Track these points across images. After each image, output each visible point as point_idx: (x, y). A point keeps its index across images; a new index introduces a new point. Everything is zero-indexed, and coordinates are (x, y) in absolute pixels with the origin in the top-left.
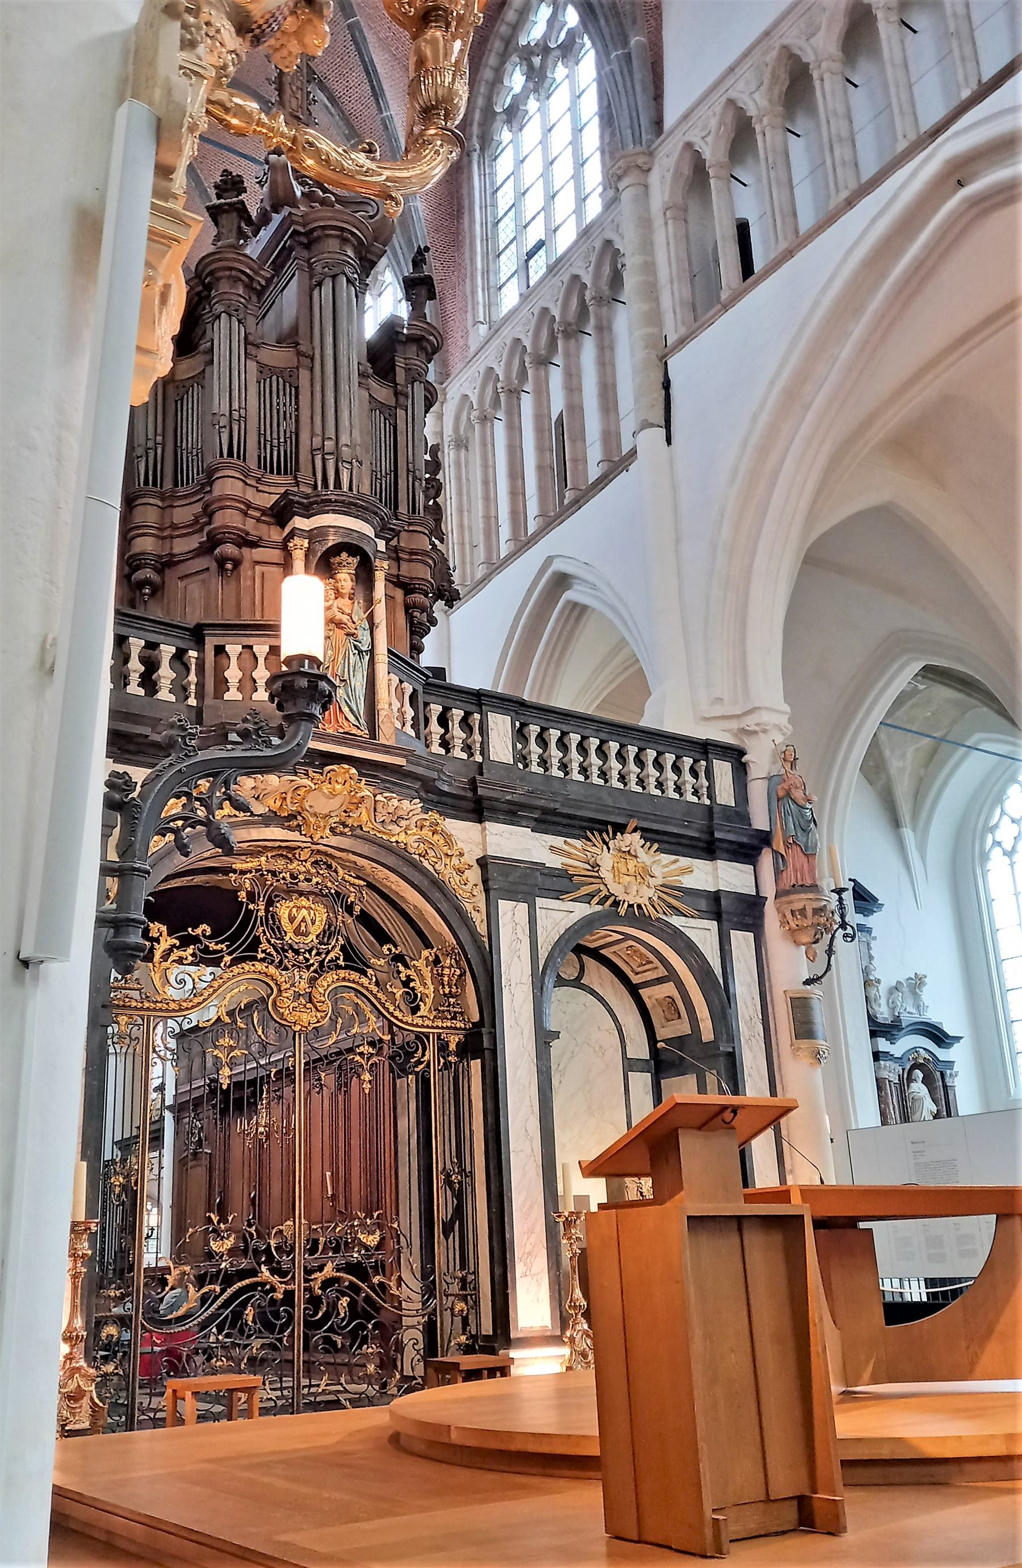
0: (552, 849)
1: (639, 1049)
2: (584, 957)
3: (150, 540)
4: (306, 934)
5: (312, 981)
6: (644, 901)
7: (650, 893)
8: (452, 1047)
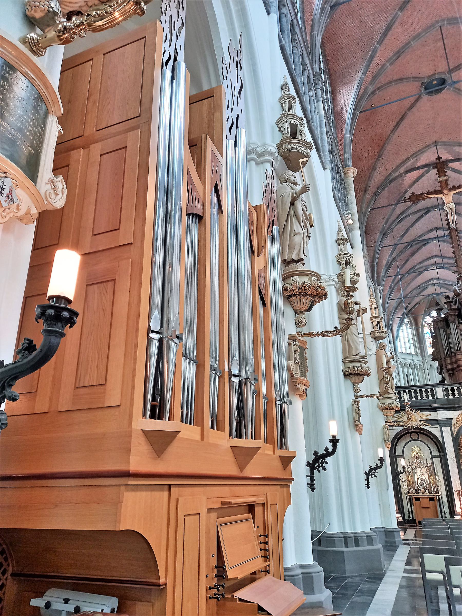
3: (450, 366)
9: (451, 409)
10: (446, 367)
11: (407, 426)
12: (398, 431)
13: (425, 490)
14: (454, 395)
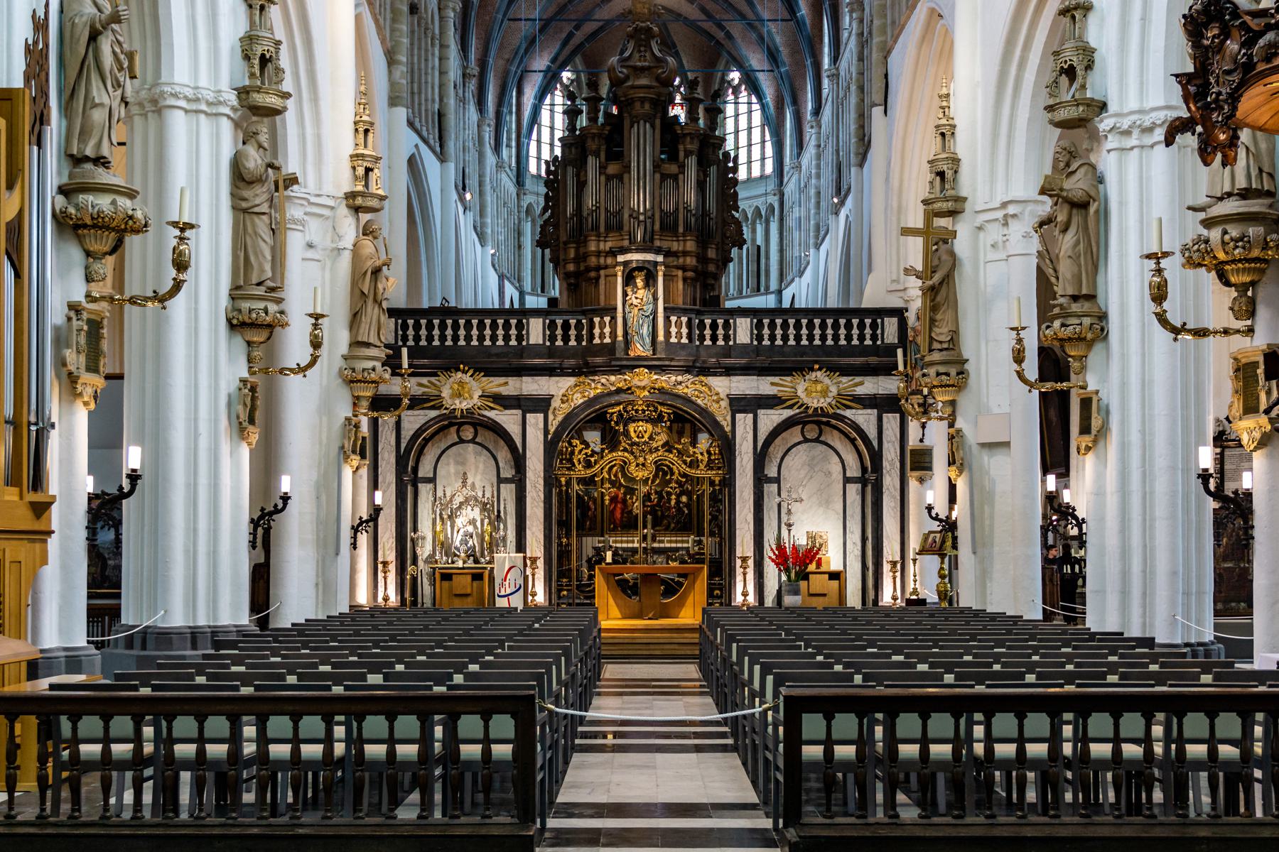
0: (772, 384)
1: (855, 471)
2: (823, 427)
4: (643, 437)
5: (645, 459)
6: (825, 405)
7: (829, 400)
8: (717, 482)
10: (564, 267)
11: (446, 409)
12: (427, 419)
13: (468, 557)
14: (566, 338)
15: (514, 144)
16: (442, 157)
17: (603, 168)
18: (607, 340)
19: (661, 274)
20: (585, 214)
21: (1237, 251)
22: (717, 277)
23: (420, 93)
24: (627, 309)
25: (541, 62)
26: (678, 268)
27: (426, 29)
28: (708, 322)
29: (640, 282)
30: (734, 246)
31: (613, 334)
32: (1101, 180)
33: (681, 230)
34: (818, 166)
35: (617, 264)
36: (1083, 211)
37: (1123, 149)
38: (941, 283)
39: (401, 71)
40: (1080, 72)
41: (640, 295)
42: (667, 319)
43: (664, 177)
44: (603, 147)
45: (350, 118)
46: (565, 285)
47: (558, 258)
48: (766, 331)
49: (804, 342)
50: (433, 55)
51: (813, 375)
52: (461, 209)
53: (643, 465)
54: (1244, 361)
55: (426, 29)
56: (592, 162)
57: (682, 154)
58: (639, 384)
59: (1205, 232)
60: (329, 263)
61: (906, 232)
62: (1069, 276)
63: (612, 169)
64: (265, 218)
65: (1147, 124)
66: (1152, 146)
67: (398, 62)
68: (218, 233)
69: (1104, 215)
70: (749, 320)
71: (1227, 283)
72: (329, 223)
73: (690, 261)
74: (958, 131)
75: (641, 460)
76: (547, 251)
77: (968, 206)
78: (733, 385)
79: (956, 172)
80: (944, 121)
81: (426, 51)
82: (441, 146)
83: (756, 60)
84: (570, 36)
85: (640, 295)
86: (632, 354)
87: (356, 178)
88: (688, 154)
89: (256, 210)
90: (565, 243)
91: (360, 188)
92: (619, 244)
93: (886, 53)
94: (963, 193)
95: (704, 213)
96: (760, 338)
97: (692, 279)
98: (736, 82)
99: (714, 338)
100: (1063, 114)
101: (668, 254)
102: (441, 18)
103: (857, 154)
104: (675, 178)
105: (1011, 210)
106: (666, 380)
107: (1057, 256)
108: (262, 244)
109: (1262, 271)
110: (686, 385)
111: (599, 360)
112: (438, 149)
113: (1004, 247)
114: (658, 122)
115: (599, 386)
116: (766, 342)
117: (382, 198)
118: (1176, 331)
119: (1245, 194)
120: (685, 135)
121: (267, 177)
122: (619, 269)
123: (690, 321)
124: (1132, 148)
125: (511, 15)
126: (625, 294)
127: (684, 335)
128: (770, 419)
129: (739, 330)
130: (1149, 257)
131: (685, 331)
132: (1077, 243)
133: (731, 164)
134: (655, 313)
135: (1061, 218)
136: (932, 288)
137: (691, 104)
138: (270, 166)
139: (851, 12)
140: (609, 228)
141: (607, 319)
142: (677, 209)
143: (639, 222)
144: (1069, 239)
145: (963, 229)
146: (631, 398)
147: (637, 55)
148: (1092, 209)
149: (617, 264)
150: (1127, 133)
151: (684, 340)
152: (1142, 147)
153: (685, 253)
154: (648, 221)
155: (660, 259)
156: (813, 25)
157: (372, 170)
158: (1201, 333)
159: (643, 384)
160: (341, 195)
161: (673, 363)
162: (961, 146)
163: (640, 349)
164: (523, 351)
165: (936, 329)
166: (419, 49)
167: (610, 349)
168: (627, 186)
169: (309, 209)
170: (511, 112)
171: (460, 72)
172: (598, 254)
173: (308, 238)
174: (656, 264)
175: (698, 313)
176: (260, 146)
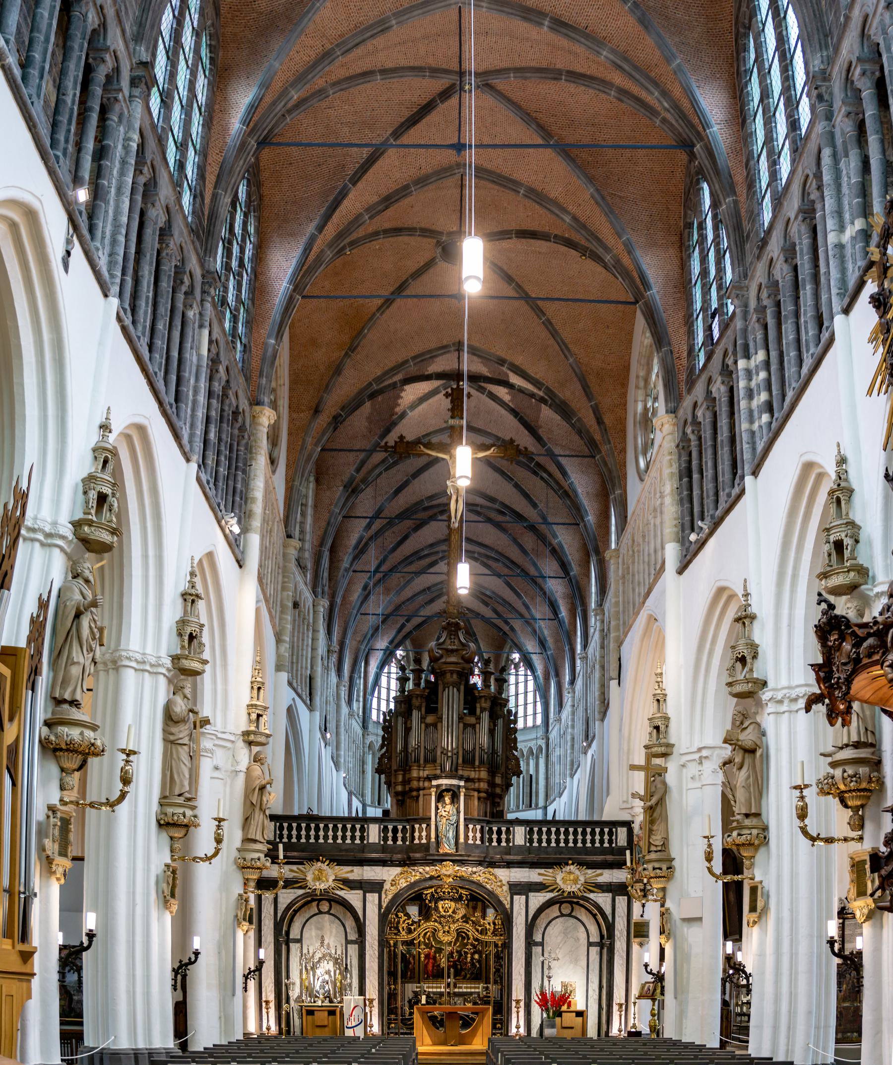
0: (539, 874)
9: (383, 863)
15: (361, 699)
16: (311, 708)
17: (423, 719)
18: (424, 841)
19: (462, 794)
20: (410, 751)
21: (852, 784)
22: (501, 797)
23: (297, 663)
24: (438, 819)
25: (382, 643)
26: (474, 790)
27: (304, 619)
28: (495, 829)
29: (447, 800)
30: (514, 775)
31: (428, 837)
32: (764, 734)
33: (477, 763)
34: (573, 720)
35: (432, 787)
36: (752, 755)
37: (778, 713)
38: (657, 804)
39: (285, 647)
40: (749, 660)
41: (447, 809)
42: (466, 826)
43: (466, 726)
44: (424, 704)
45: (249, 679)
46: (395, 801)
47: (390, 782)
48: (535, 836)
49: (562, 844)
50: (308, 636)
51: (568, 868)
52: (323, 745)
53: (448, 932)
54: (857, 859)
55: (304, 619)
56: (415, 713)
57: (478, 710)
58: (446, 873)
59: (831, 771)
60: (229, 781)
61: (633, 768)
62: (743, 800)
63: (430, 719)
64: (185, 747)
65: (793, 696)
66: (797, 711)
67: (284, 641)
68: (152, 757)
69: (766, 757)
70: (523, 828)
71: (846, 806)
72: (231, 752)
73: (483, 786)
74: (668, 698)
75: (447, 928)
76: (383, 776)
77: (675, 750)
78: (512, 874)
79: (667, 726)
80: (659, 692)
81: (303, 633)
82: (310, 700)
83: (531, 646)
84: (403, 626)
85: (447, 809)
86: (441, 851)
87: (250, 721)
88: (483, 710)
89: (180, 742)
90: (396, 771)
91: (253, 728)
92: (434, 772)
93: (620, 644)
94: (672, 741)
95: (494, 752)
96: (531, 841)
97: (484, 798)
98: (517, 660)
99: (499, 841)
100: (738, 689)
101: (468, 780)
102: (314, 612)
103: (600, 712)
104: (473, 726)
105: (704, 753)
106: (465, 871)
107: (735, 786)
108: (183, 766)
109: (868, 798)
110: (479, 874)
111: (418, 855)
112: (308, 702)
113: (700, 779)
114: (462, 687)
115: (418, 874)
116: (535, 844)
117: (268, 736)
118: (813, 839)
119: (857, 745)
120: (481, 697)
121: (189, 718)
122: (433, 790)
123: (482, 828)
124: (784, 713)
125: (362, 611)
126: (437, 808)
127: (478, 838)
128: (537, 899)
129: (516, 835)
130: (795, 788)
131: (478, 835)
132: (748, 777)
133: (512, 718)
134: (458, 822)
135: (738, 760)
136: (651, 807)
137: (486, 675)
138: (191, 711)
139: (596, 615)
140: (426, 761)
141: (424, 826)
142: (475, 748)
143: (448, 757)
144: (743, 773)
145: (672, 766)
146: (440, 883)
147: (448, 641)
148: (758, 753)
149: (432, 787)
150: (780, 702)
151: (478, 842)
152: (791, 712)
153: (480, 780)
154: (454, 757)
155: (462, 783)
156: (570, 623)
157: (262, 716)
158: (829, 840)
159: (448, 873)
160: (240, 733)
161: (470, 859)
162: (671, 708)
163: (447, 848)
164: (364, 847)
165: (653, 837)
166: (299, 632)
167: (427, 847)
168: (439, 731)
169: (217, 742)
170: (360, 677)
171: (326, 649)
172: (419, 779)
173: (215, 763)
174: (459, 787)
175: (488, 822)
176: (185, 697)
